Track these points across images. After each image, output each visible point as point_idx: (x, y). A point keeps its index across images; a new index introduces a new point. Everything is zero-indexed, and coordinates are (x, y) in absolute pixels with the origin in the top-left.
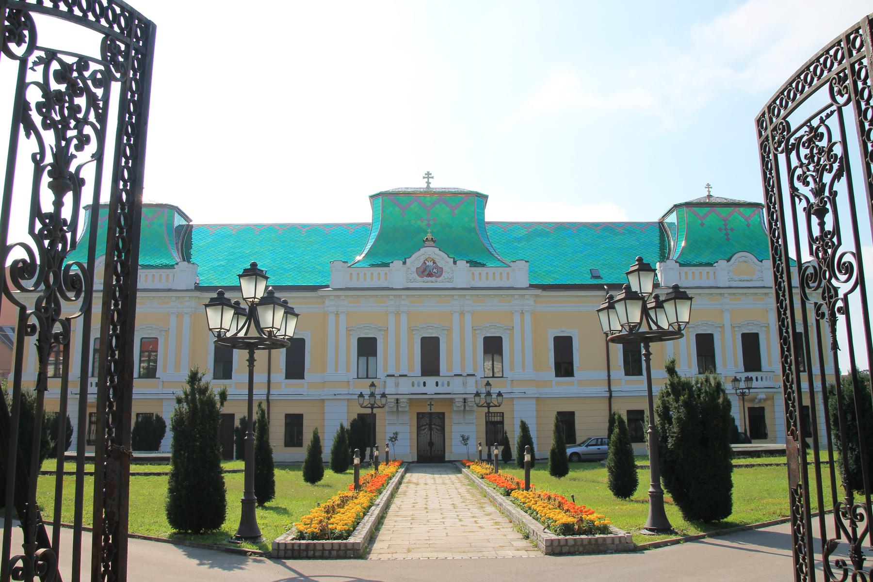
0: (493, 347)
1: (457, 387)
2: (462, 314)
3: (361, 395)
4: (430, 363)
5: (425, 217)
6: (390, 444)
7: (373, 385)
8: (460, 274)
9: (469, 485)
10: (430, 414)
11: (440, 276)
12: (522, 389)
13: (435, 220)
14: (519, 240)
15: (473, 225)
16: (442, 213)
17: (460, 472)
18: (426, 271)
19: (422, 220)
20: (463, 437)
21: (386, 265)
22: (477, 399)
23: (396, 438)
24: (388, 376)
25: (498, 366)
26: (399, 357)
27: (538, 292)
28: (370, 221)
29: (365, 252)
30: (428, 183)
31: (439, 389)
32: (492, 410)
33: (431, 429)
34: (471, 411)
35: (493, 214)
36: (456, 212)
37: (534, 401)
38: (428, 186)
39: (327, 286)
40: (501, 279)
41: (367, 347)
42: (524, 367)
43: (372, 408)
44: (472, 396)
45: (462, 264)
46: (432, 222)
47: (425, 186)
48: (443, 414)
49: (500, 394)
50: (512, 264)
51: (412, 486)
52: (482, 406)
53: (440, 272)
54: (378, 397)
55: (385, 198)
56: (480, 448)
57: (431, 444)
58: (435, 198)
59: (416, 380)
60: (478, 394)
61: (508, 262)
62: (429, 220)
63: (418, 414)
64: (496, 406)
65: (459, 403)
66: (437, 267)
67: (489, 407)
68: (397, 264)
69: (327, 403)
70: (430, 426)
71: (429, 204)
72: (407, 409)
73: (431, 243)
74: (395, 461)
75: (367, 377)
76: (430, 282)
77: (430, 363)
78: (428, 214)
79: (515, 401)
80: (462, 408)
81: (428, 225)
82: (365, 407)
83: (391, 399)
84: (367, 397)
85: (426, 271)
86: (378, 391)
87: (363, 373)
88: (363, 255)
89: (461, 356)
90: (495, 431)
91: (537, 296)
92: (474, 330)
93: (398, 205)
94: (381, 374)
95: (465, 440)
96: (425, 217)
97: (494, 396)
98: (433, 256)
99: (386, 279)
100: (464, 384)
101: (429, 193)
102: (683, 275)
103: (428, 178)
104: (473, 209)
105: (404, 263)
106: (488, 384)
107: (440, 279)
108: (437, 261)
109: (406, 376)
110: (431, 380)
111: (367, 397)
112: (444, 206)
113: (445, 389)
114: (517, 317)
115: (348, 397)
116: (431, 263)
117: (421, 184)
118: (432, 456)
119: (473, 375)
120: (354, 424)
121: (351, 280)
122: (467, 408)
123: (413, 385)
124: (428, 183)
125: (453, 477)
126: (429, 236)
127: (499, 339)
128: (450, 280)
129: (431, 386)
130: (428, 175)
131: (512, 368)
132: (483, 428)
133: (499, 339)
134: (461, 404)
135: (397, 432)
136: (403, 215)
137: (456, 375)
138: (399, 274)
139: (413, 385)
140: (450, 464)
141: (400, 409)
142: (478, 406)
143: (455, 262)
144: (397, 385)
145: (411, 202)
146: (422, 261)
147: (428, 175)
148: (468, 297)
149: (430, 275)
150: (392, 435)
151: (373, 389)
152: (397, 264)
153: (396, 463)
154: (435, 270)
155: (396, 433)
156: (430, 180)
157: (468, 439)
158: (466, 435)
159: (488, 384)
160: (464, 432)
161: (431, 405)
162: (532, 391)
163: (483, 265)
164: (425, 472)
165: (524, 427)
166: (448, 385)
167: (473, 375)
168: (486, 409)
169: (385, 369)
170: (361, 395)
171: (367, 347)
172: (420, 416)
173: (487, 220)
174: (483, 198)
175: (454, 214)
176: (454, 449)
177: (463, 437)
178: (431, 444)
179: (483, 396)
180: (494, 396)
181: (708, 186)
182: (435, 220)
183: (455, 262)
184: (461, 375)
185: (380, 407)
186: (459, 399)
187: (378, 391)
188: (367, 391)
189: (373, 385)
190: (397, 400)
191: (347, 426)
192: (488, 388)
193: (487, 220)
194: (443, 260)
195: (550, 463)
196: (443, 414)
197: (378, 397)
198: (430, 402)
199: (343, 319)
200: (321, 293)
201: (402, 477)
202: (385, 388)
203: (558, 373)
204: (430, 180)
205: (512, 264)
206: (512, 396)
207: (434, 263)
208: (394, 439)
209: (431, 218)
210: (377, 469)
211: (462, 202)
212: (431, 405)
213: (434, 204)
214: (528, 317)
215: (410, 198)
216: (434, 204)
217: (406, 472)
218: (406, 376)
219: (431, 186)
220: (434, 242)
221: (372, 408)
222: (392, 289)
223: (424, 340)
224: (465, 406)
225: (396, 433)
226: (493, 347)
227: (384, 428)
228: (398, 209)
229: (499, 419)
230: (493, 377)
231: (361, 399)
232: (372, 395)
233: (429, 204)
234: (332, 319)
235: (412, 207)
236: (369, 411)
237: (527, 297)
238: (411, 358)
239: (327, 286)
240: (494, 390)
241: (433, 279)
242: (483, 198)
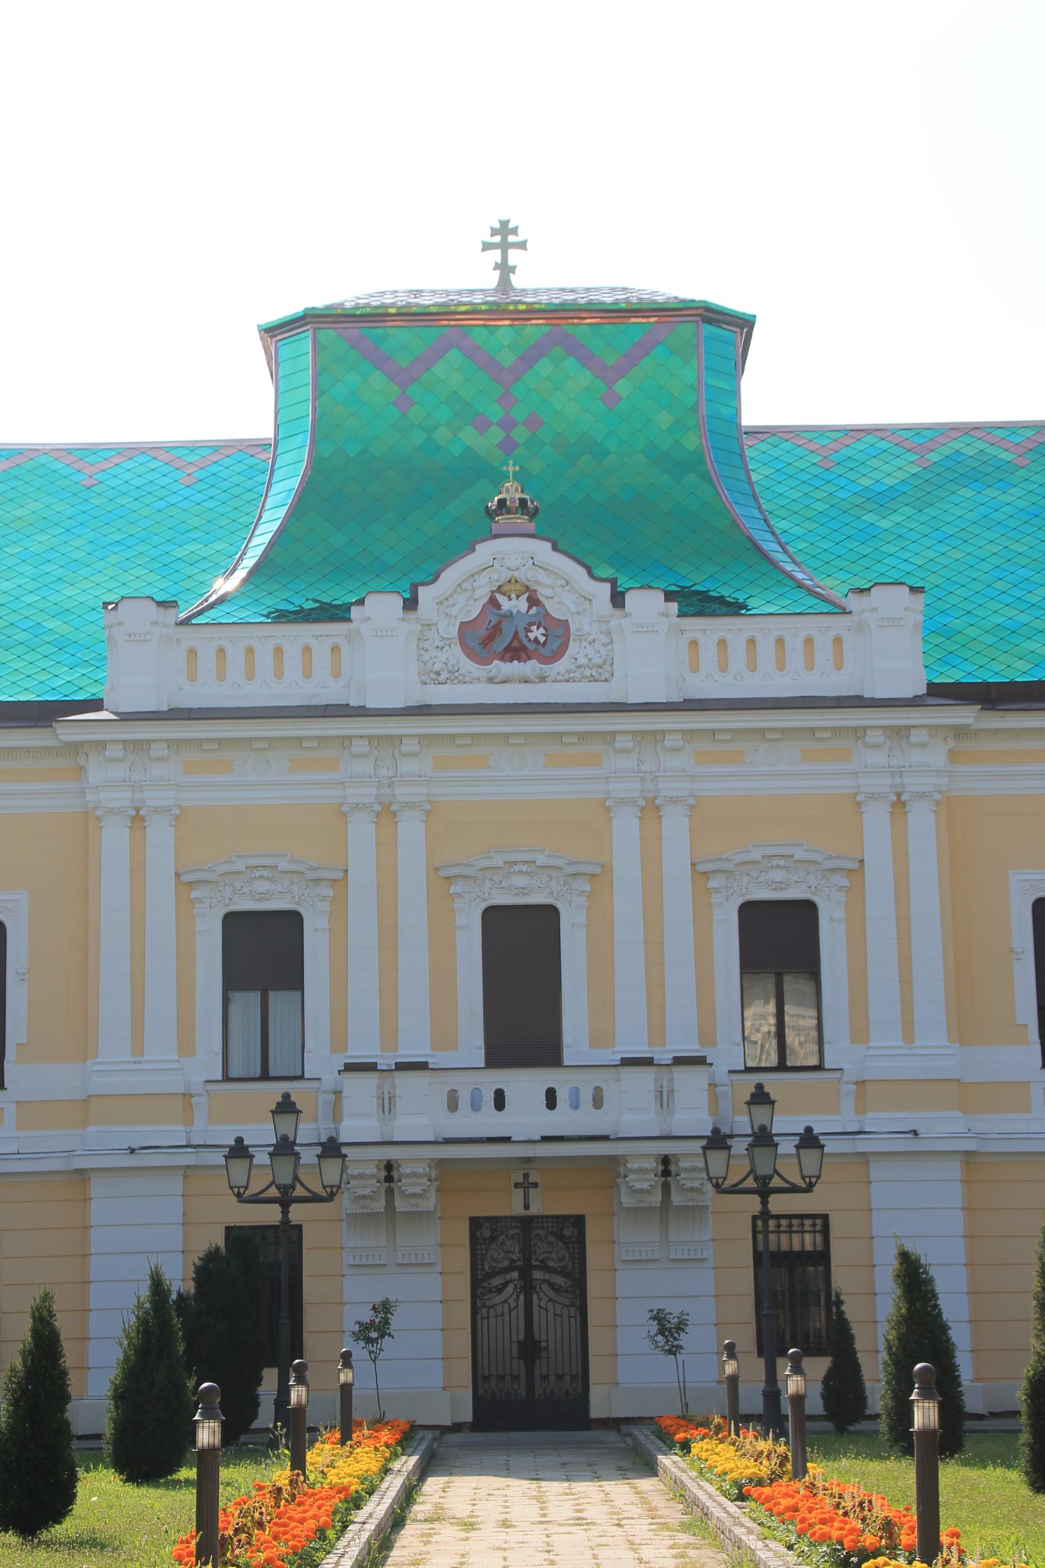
0: (780, 942)
1: (632, 1109)
2: (651, 809)
3: (239, 1150)
4: (522, 1016)
5: (495, 412)
6: (360, 1351)
7: (286, 1107)
8: (641, 646)
9: (685, 1527)
10: (527, 1223)
11: (557, 655)
12: (906, 1119)
13: (533, 422)
14: (883, 500)
15: (691, 442)
16: (564, 394)
17: (650, 1468)
18: (504, 636)
19: (481, 424)
20: (659, 1317)
21: (337, 613)
22: (717, 1159)
23: (383, 1328)
24: (350, 1068)
26: (395, 986)
27: (966, 715)
28: (267, 432)
29: (249, 562)
30: (505, 269)
31: (562, 1120)
32: (778, 1204)
33: (528, 1288)
34: (694, 1212)
36: (622, 387)
37: (954, 1169)
38: (505, 283)
39: (96, 704)
40: (810, 665)
41: (264, 952)
43: (285, 1202)
44: (697, 1146)
45: (647, 605)
46: (520, 434)
47: (491, 280)
48: (578, 1222)
49: (809, 1140)
50: (853, 603)
51: (447, 1533)
52: (735, 1190)
53: (556, 639)
54: (308, 1156)
55: (327, 335)
56: (730, 1368)
57: (530, 1348)
58: (535, 330)
59: (464, 1085)
60: (717, 1141)
61: (838, 593)
62: (507, 424)
63: (475, 1223)
64: (794, 1189)
66: (545, 620)
67: (764, 1192)
68: (382, 608)
69: (97, 1187)
70: (526, 1271)
71: (507, 359)
72: (429, 1203)
73: (521, 521)
74: (378, 1423)
75: (265, 1076)
77: (522, 1016)
78: (506, 400)
79: (877, 1171)
80: (656, 1199)
81: (508, 446)
82: (256, 1199)
83: (364, 1163)
84: (262, 1158)
85: (504, 636)
86: (308, 1132)
87: (244, 1060)
88: (241, 574)
89: (650, 981)
90: (793, 1296)
91: (960, 732)
92: (700, 875)
93: (381, 361)
94: (321, 1061)
95: (669, 1330)
96: (495, 412)
97: (787, 1147)
98: (525, 575)
99: (336, 673)
100: (664, 1098)
101: (505, 310)
103: (504, 247)
104: (689, 375)
105: (411, 604)
106: (760, 1098)
107: (560, 666)
108: (543, 593)
109: (422, 1066)
110: (525, 1085)
111: (262, 1158)
112: (571, 363)
114: (877, 821)
115: (189, 1159)
116: (522, 604)
117: (471, 276)
118: (533, 1405)
119: (700, 1061)
120: (209, 1270)
121: (192, 677)
122: (677, 1199)
123: (453, 1104)
124: (505, 269)
125: (619, 1492)
126: (511, 492)
127: (804, 913)
129: (524, 1108)
130: (504, 237)
131: (860, 1033)
132: (745, 1279)
133: (804, 913)
134: (650, 1181)
135: (392, 1303)
136: (403, 403)
137: (628, 1062)
138: (389, 650)
140: (610, 1436)
141: (400, 1205)
142: (717, 1186)
143: (618, 599)
144: (387, 1104)
145: (437, 352)
146: (483, 594)
147: (504, 237)
148: (671, 741)
149: (516, 651)
150: (367, 1316)
151: (286, 1124)
152: (382, 608)
153: (385, 1436)
154: (537, 633)
155: (385, 1308)
156: (514, 256)
157: (681, 1326)
158: (673, 1309)
159: (760, 1098)
160: (666, 1296)
161: (526, 1185)
162: (946, 1126)
163: (735, 608)
164: (507, 1471)
165: (913, 1278)
166: (598, 1101)
167: (700, 1061)
168: (754, 1203)
169: (339, 1042)
170: (239, 1150)
171: (264, 952)
172: (483, 1232)
173: (749, 418)
175: (611, 399)
176: (625, 1372)
177: (659, 1317)
178: (530, 1348)
179: (739, 1147)
180: (787, 1147)
182: (533, 422)
183: (618, 599)
184: (648, 1062)
185: (315, 1199)
186: (643, 1159)
187: (308, 1132)
188: (261, 1134)
189: (286, 1107)
190: (389, 1166)
191: (180, 1280)
192: (761, 1114)
193: (749, 418)
194: (570, 588)
195: (1025, 1437)
196: (578, 1222)
197: (308, 1156)
198: (526, 1174)
199: (160, 836)
200: (66, 731)
201: (408, 1495)
202: (337, 1115)
204: (514, 256)
205: (853, 603)
206: (862, 1145)
207: (533, 601)
208: (376, 1329)
209: (519, 413)
210: (298, 1463)
211: (643, 348)
212: (526, 1185)
213: (529, 359)
214: (922, 820)
215: (431, 334)
216: (529, 359)
217: (423, 1471)
218: (422, 1066)
219: (518, 281)
220: (533, 514)
221: (285, 1202)
222: (362, 712)
223: (499, 922)
224: (666, 1188)
225: (385, 1308)
226: (780, 942)
227: (340, 1278)
228: (378, 380)
229: (809, 1242)
230: (782, 1066)
231: (239, 1167)
232: (285, 1148)
233: (507, 359)
234: (115, 838)
235: (440, 368)
236: (270, 1215)
237: (916, 736)
238: (446, 997)
239: (96, 704)
240: (786, 1123)
241: (530, 667)
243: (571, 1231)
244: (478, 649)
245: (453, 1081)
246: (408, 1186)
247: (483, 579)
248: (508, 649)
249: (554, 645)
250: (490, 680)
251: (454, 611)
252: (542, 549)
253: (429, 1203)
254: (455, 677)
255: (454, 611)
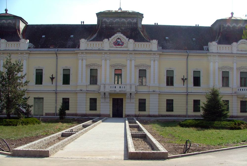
8: (131, 44)
18: (117, 44)
25: (144, 80)
35: (145, 22)
42: (154, 81)
65: (128, 95)
66: (122, 42)
76: (119, 48)
85: (117, 44)
102: (219, 47)
107: (123, 46)
108: (121, 39)
113: (124, 89)
128: (127, 47)
139: (111, 88)
146: (116, 39)
149: (119, 45)
154: (121, 43)
174: (140, 16)
181: (232, 14)
194: (124, 38)
196: (123, 98)
198: (118, 94)
203: (168, 84)
207: (121, 40)
241: (120, 46)
242: (140, 16)
243: (122, 100)
244: (115, 44)
245: (111, 85)
246: (106, 95)
247: (116, 38)
248: (118, 45)
249: (122, 44)
250: (116, 47)
251: (113, 41)
252: (122, 35)
253: (109, 97)
254: (113, 47)
255: (113, 41)
